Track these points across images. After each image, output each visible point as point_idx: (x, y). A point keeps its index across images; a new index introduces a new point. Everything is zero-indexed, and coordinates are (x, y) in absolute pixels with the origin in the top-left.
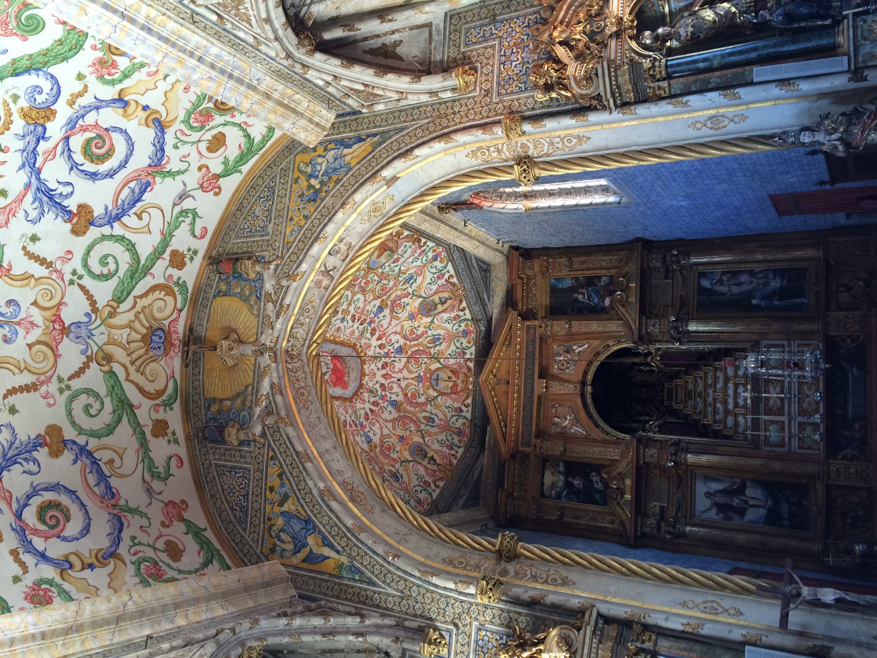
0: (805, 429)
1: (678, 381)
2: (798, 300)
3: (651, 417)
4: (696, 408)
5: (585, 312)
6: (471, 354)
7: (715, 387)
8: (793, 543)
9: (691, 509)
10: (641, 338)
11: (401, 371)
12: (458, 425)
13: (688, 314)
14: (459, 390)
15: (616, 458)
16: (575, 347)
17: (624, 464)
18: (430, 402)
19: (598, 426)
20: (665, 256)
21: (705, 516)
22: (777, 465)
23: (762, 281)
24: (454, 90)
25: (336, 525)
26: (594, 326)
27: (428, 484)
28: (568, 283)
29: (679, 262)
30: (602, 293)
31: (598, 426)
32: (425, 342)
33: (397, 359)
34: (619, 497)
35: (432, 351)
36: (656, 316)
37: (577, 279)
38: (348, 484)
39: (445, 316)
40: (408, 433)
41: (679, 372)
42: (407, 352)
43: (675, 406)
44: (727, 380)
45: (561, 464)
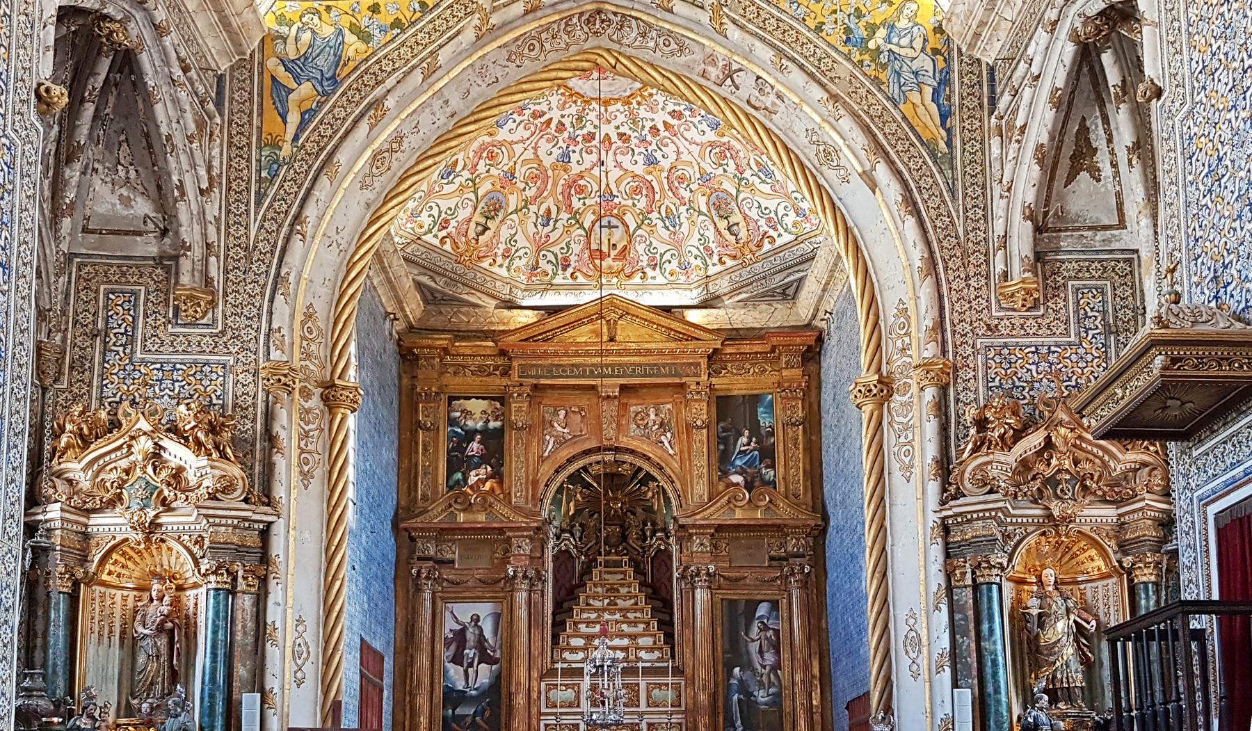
11: (619, 165)
12: (542, 264)
17: (506, 511)
18: (575, 218)
24: (1005, 275)
25: (335, 132)
26: (701, 462)
27: (445, 225)
32: (667, 202)
35: (654, 215)
38: (400, 144)
39: (711, 234)
40: (522, 186)
42: (650, 173)
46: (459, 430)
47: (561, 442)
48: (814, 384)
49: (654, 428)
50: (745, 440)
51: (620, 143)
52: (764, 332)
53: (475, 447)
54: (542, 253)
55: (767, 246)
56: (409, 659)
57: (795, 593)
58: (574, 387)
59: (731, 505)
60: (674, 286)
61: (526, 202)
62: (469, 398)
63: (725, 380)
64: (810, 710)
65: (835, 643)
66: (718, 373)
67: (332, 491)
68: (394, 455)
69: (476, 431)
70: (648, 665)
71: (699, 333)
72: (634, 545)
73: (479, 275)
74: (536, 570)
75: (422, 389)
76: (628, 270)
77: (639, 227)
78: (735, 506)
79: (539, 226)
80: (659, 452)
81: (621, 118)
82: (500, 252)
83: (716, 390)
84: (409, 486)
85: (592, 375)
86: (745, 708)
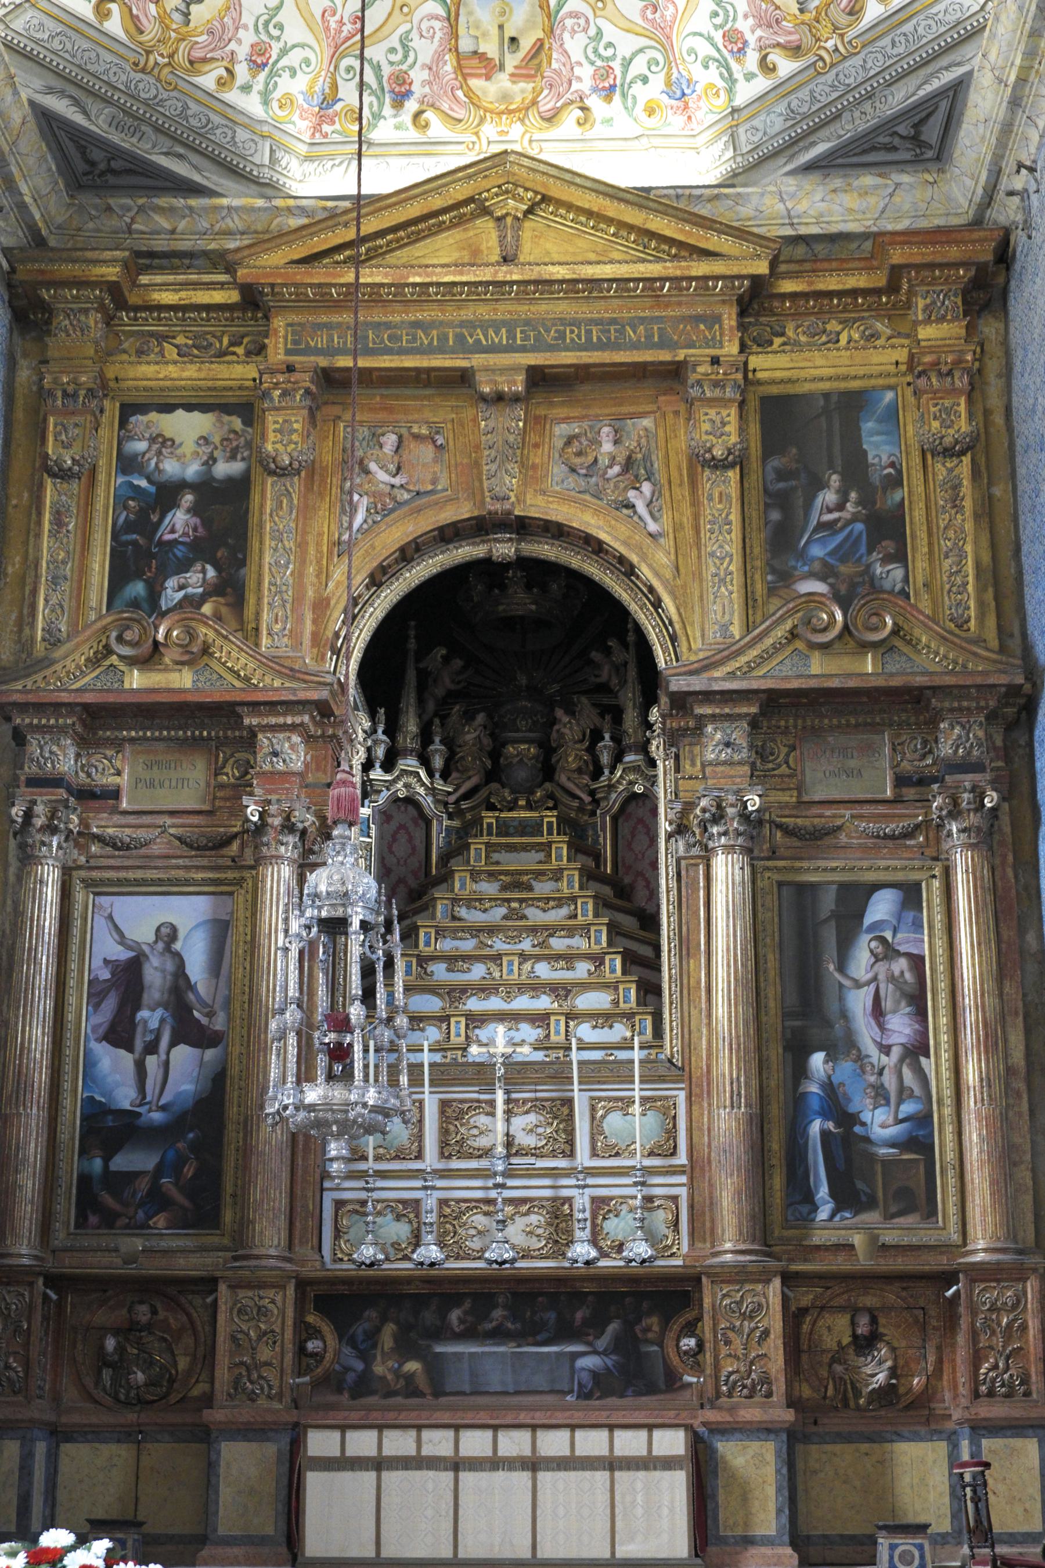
0: (398, 1218)
1: (561, 848)
2: (823, 1192)
3: (445, 776)
4: (470, 903)
5: (775, 516)
6: (608, 121)
9: (120, 882)
10: (681, 702)
13: (773, 855)
14: (474, 83)
15: (265, 641)
16: (646, 488)
19: (377, 580)
20: (977, 767)
23: (889, 1081)
29: (955, 813)
30: (844, 569)
31: (377, 580)
34: (126, 651)
36: (761, 753)
37: (896, 481)
43: (477, 846)
45: (236, 468)
48: (993, 367)
60: (656, 141)
63: (782, 361)
66: (764, 343)
72: (570, 786)
80: (623, 530)
83: (759, 383)
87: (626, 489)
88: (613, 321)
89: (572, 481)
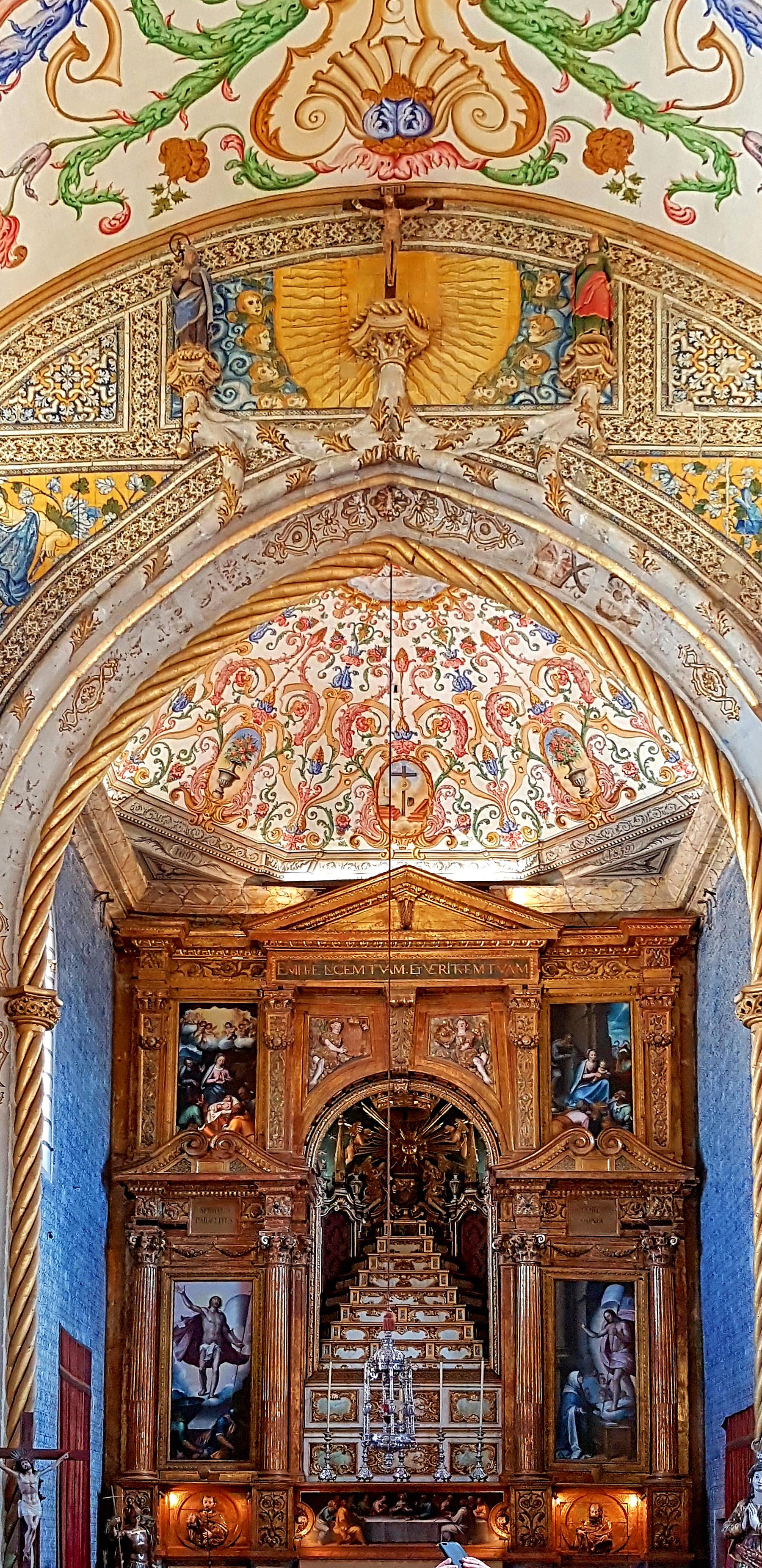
1: (430, 1240)
4: (378, 1276)
7: (418, 1310)
8: (145, 1437)
11: (418, 691)
17: (258, 1159)
21: (178, 1296)
22: (277, 1411)
27: (176, 773)
28: (617, 1037)
33: (442, 681)
41: (449, 1245)
44: (431, 1329)
46: (195, 1050)
47: (334, 1066)
49: (463, 1048)
50: (589, 1064)
51: (419, 661)
52: (617, 918)
53: (216, 1072)
54: (310, 810)
55: (624, 801)
56: (126, 1356)
57: (657, 1273)
58: (352, 991)
59: (570, 1153)
60: (492, 855)
61: (290, 740)
62: (208, 1006)
63: (563, 983)
64: (674, 1428)
65: (710, 1341)
66: (553, 972)
67: (20, 1135)
68: (106, 1083)
69: (217, 1051)
70: (452, 1366)
71: (527, 919)
73: (223, 840)
74: (299, 1238)
75: (144, 993)
76: (428, 834)
77: (445, 775)
78: (576, 1154)
79: (307, 775)
80: (470, 1080)
81: (422, 627)
82: (252, 809)
83: (550, 996)
84: (126, 1125)
85: (378, 975)
86: (584, 1425)
87: (472, 1057)
88: (466, 961)
89: (440, 1052)
